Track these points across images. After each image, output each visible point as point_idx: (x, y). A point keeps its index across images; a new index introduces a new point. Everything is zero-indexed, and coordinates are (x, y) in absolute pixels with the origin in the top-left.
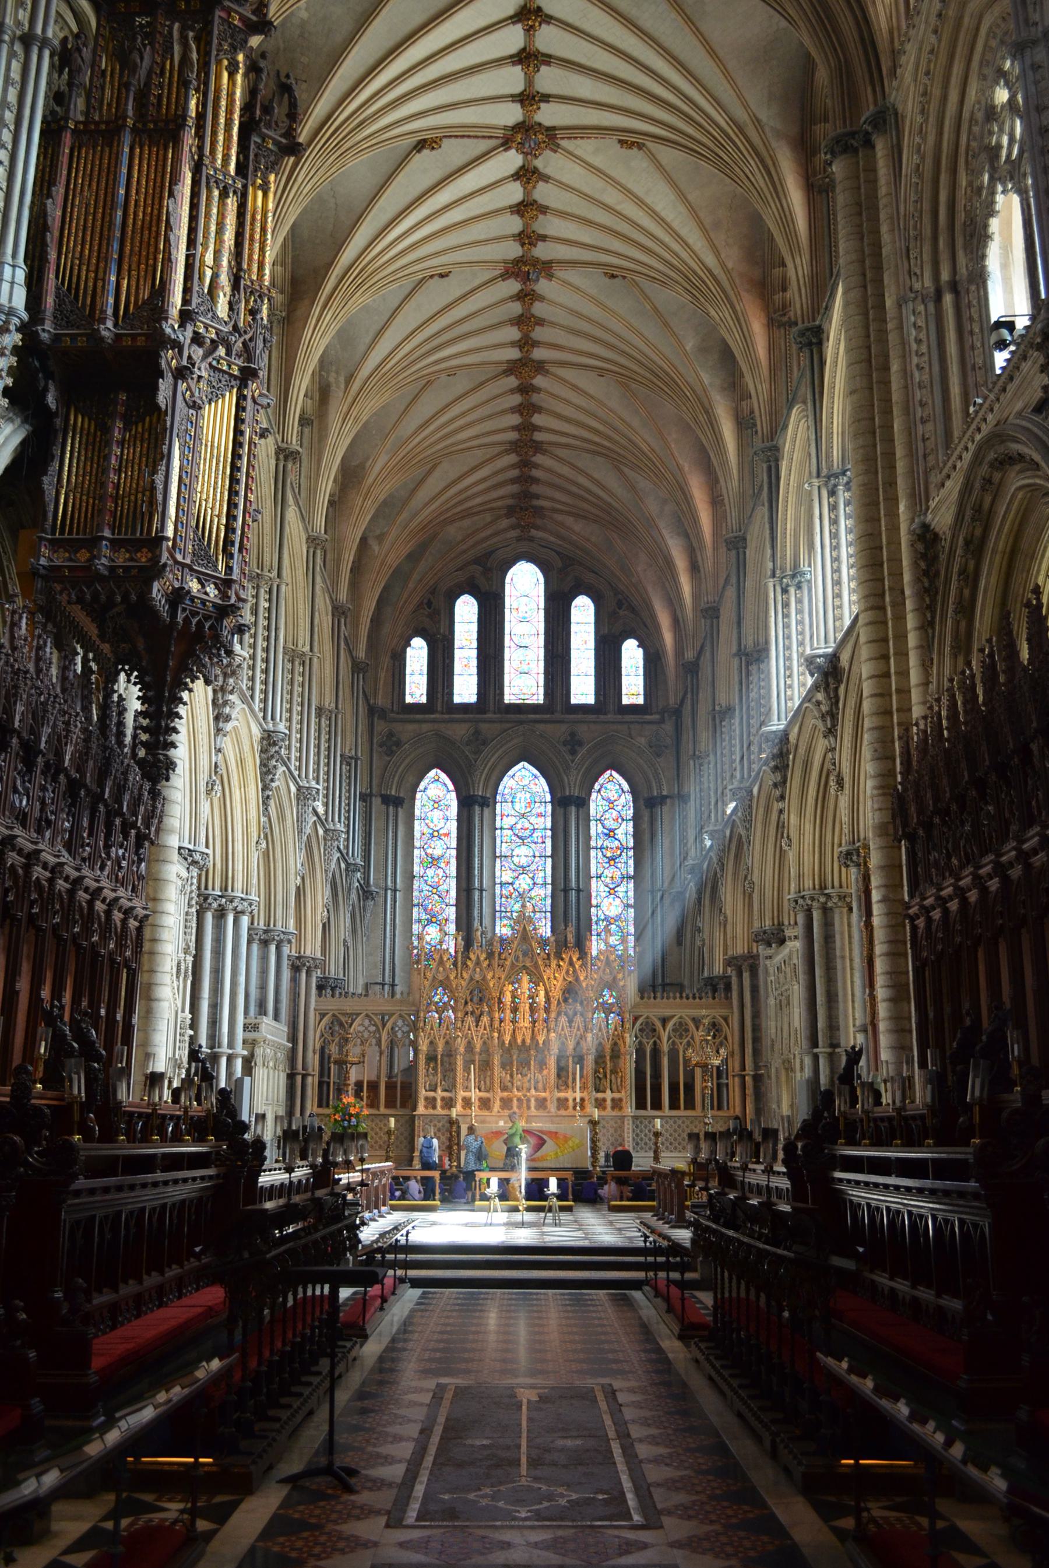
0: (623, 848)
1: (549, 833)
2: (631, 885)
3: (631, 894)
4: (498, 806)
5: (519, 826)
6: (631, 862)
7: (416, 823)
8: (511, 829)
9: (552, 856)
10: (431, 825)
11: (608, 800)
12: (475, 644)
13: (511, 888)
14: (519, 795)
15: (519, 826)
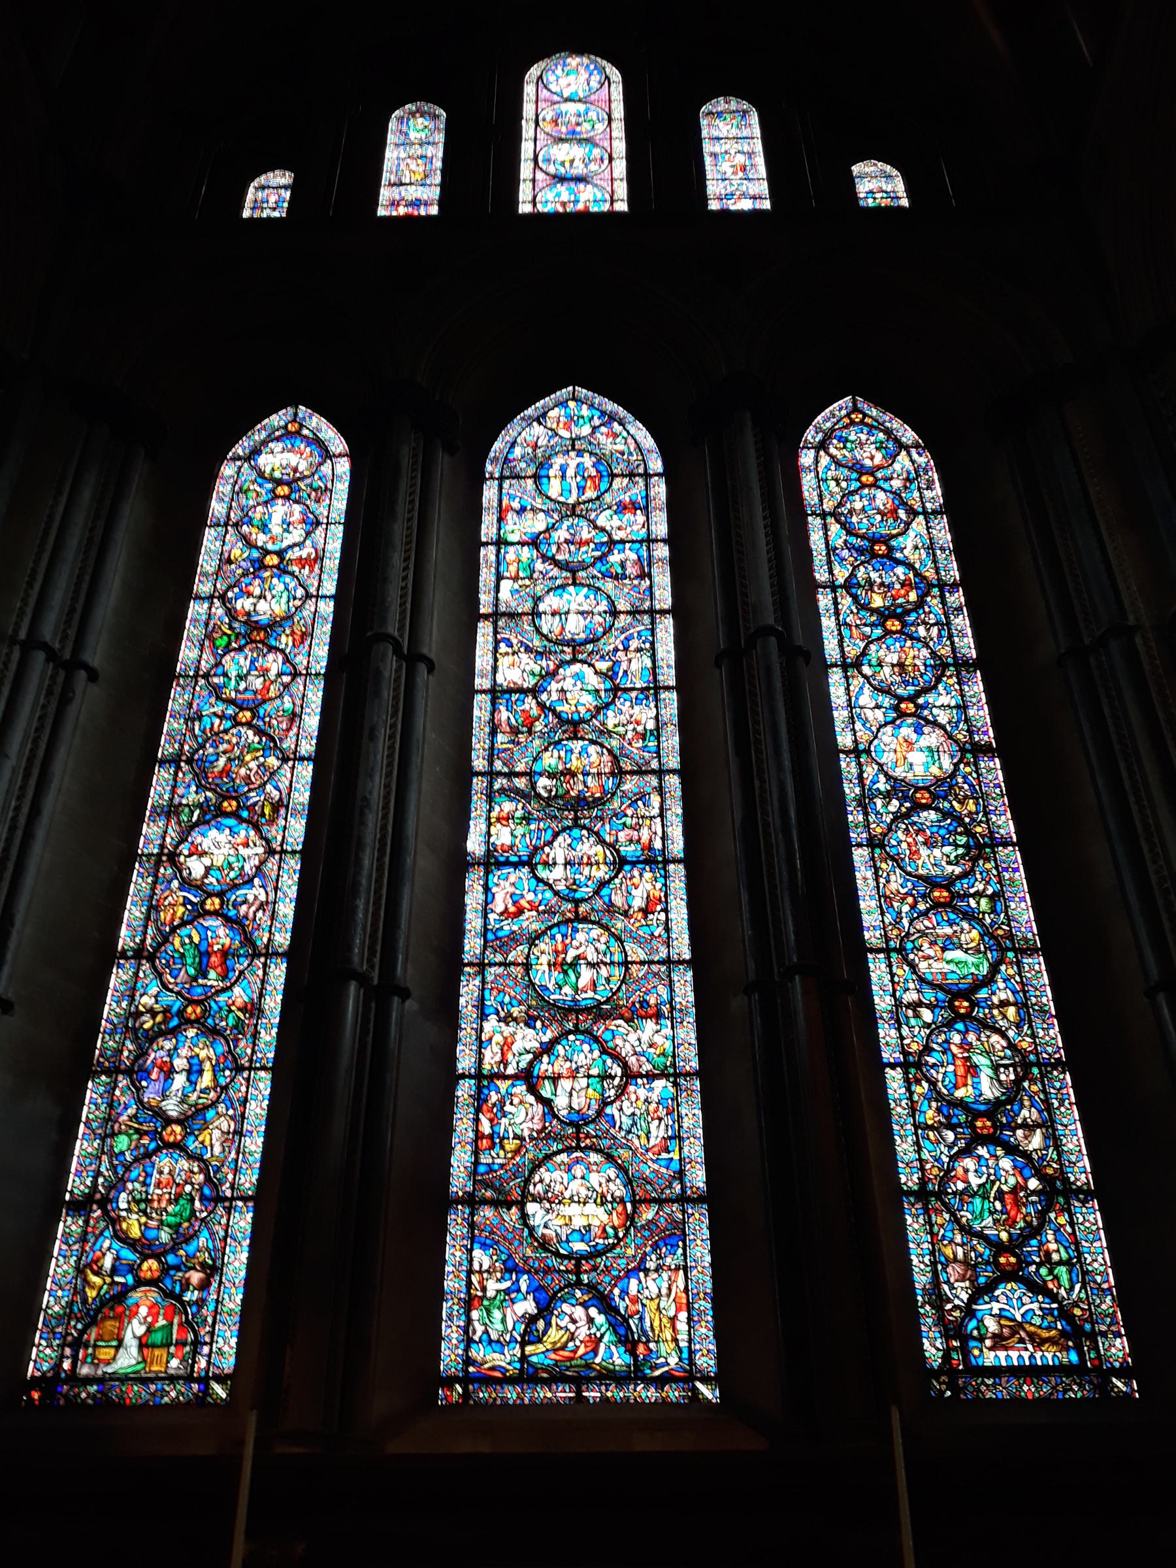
0: (924, 587)
1: (662, 551)
2: (976, 688)
3: (981, 714)
4: (489, 493)
5: (561, 534)
6: (962, 622)
7: (210, 534)
8: (534, 542)
9: (677, 611)
10: (261, 539)
11: (858, 468)
12: (438, 179)
13: (530, 704)
14: (558, 461)
15: (561, 534)
